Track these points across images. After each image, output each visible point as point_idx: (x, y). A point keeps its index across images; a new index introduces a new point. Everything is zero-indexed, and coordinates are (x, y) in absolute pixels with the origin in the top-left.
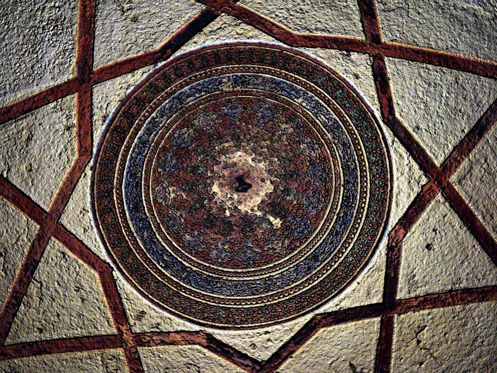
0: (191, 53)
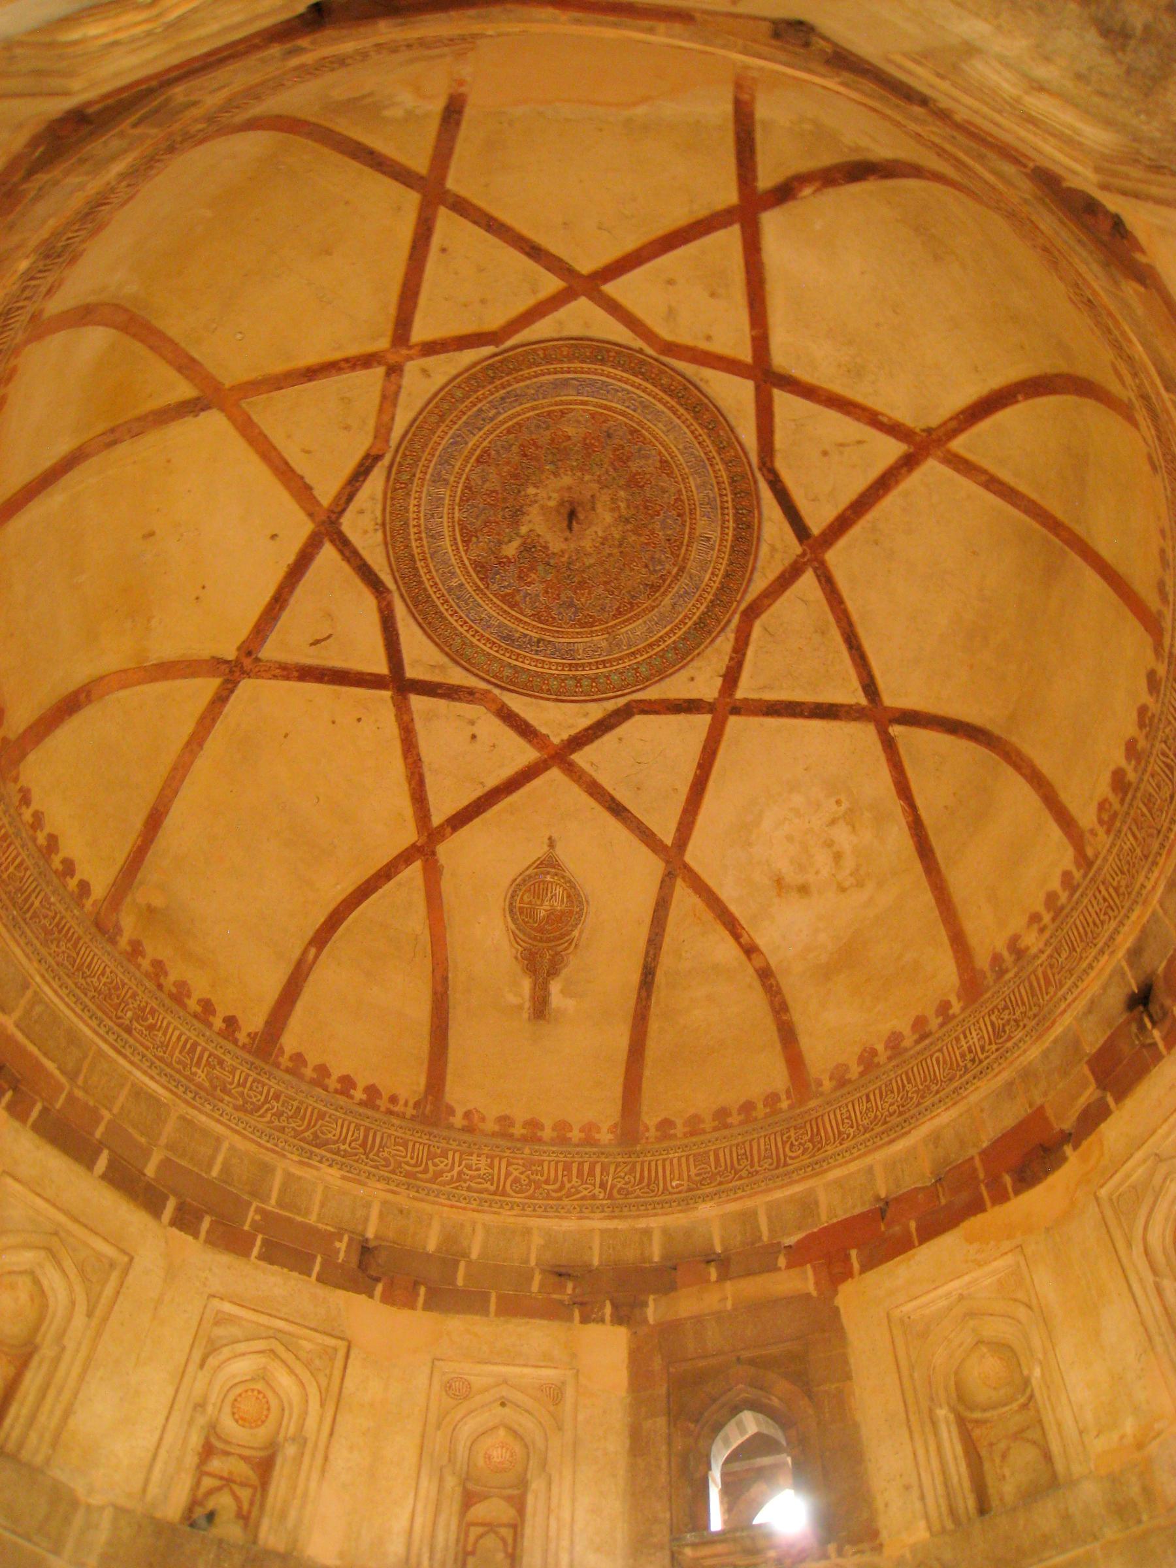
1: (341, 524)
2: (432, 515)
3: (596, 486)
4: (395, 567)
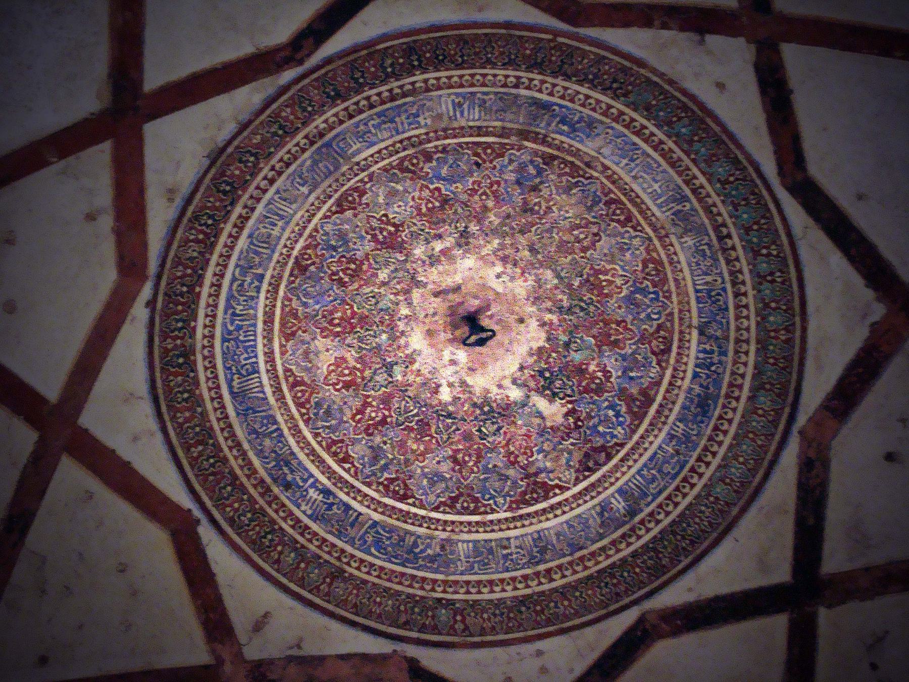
0: (355, 49)
2: (505, 557)
3: (416, 294)
4: (604, 612)
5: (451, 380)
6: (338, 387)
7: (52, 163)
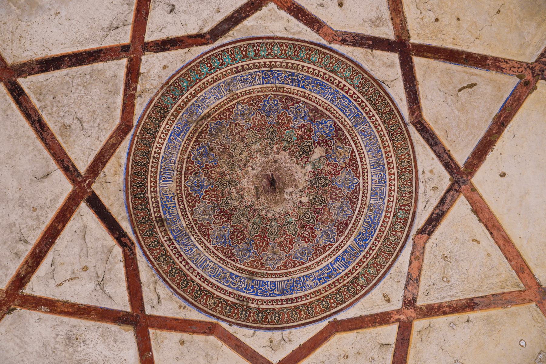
1: (450, 180)
3: (256, 207)
5: (298, 196)
6: (291, 247)
7: (152, 355)
